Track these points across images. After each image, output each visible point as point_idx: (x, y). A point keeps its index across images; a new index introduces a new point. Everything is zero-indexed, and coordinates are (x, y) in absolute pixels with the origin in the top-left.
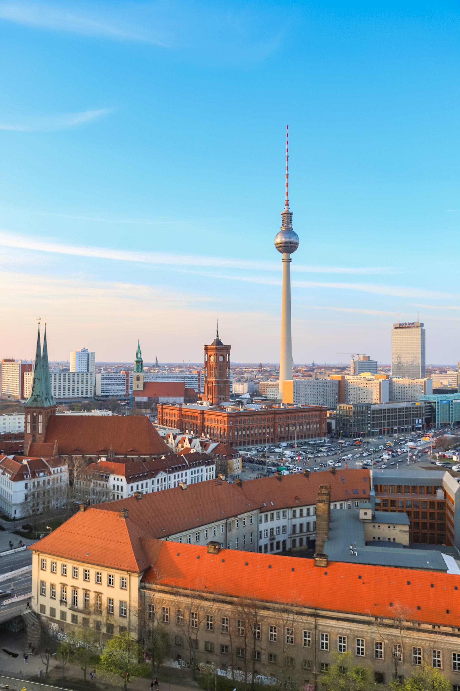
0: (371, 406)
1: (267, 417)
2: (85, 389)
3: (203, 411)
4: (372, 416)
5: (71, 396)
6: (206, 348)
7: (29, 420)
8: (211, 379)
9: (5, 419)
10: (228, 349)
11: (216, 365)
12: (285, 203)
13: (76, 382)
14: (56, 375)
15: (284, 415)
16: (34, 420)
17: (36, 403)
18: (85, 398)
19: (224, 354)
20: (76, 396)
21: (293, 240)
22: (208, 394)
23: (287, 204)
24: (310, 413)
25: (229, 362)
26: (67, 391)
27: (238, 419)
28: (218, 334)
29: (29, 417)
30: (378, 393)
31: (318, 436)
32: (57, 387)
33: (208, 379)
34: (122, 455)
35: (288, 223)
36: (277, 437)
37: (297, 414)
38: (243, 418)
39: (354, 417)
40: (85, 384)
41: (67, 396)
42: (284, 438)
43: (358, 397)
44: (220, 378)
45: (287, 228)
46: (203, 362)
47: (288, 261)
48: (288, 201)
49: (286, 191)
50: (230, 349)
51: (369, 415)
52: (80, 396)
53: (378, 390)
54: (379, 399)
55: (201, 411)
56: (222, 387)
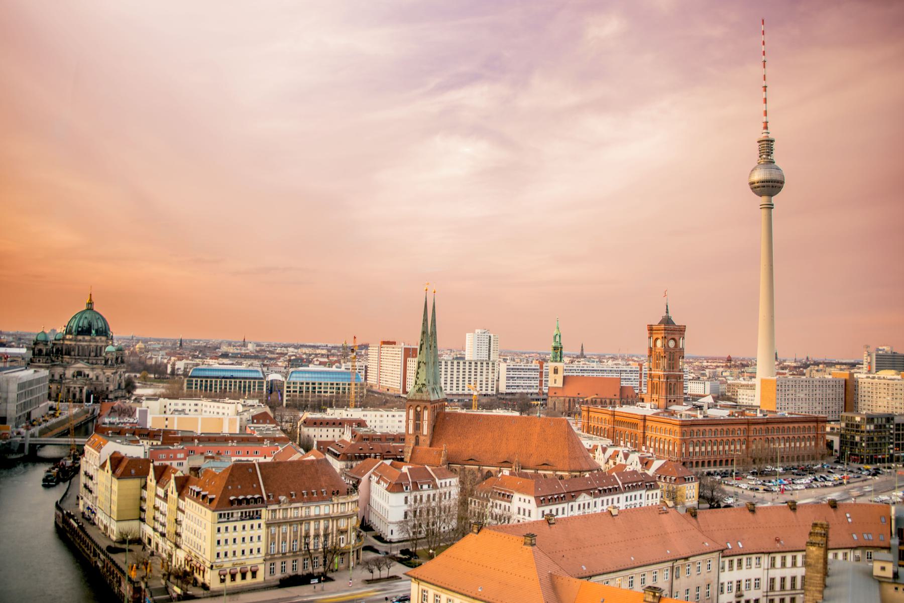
3: (645, 416)
4: (895, 432)
6: (651, 329)
8: (657, 372)
9: (381, 416)
10: (681, 330)
11: (665, 353)
12: (763, 125)
15: (762, 426)
16: (418, 416)
17: (420, 394)
18: (485, 395)
19: (676, 337)
22: (652, 393)
23: (766, 128)
24: (801, 425)
27: (695, 429)
28: (667, 309)
29: (412, 412)
33: (653, 372)
34: (532, 469)
35: (768, 154)
37: (781, 426)
38: (702, 428)
40: (484, 377)
44: (670, 371)
45: (766, 160)
48: (766, 122)
50: (685, 331)
51: (892, 432)
55: (642, 416)
56: (673, 384)
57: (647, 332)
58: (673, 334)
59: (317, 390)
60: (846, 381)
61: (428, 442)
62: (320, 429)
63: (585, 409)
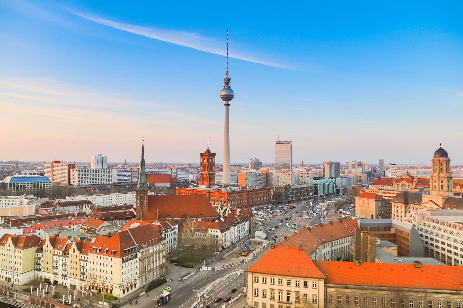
0: (292, 187)
1: (245, 193)
2: (108, 179)
3: (209, 191)
5: (100, 183)
6: (202, 155)
7: (139, 198)
9: (95, 198)
10: (214, 155)
12: (226, 73)
13: (103, 175)
14: (91, 170)
15: (252, 193)
16: (142, 198)
17: (143, 188)
18: (108, 184)
19: (212, 158)
20: (102, 183)
21: (231, 94)
22: (203, 181)
23: (227, 74)
24: (264, 191)
25: (214, 163)
26: (97, 180)
27: (232, 195)
29: (139, 196)
30: (290, 180)
31: (267, 204)
32: (92, 178)
34: (195, 217)
36: (250, 205)
37: (258, 192)
38: (234, 195)
39: (284, 192)
40: (108, 176)
41: (97, 183)
42: (252, 205)
43: (278, 182)
46: (200, 163)
47: (228, 105)
49: (227, 66)
52: (105, 183)
53: (290, 178)
54: (290, 183)
57: (200, 156)
58: (211, 157)
59: (26, 186)
60: (266, 173)
61: (147, 209)
62: (69, 207)
63: (178, 189)
